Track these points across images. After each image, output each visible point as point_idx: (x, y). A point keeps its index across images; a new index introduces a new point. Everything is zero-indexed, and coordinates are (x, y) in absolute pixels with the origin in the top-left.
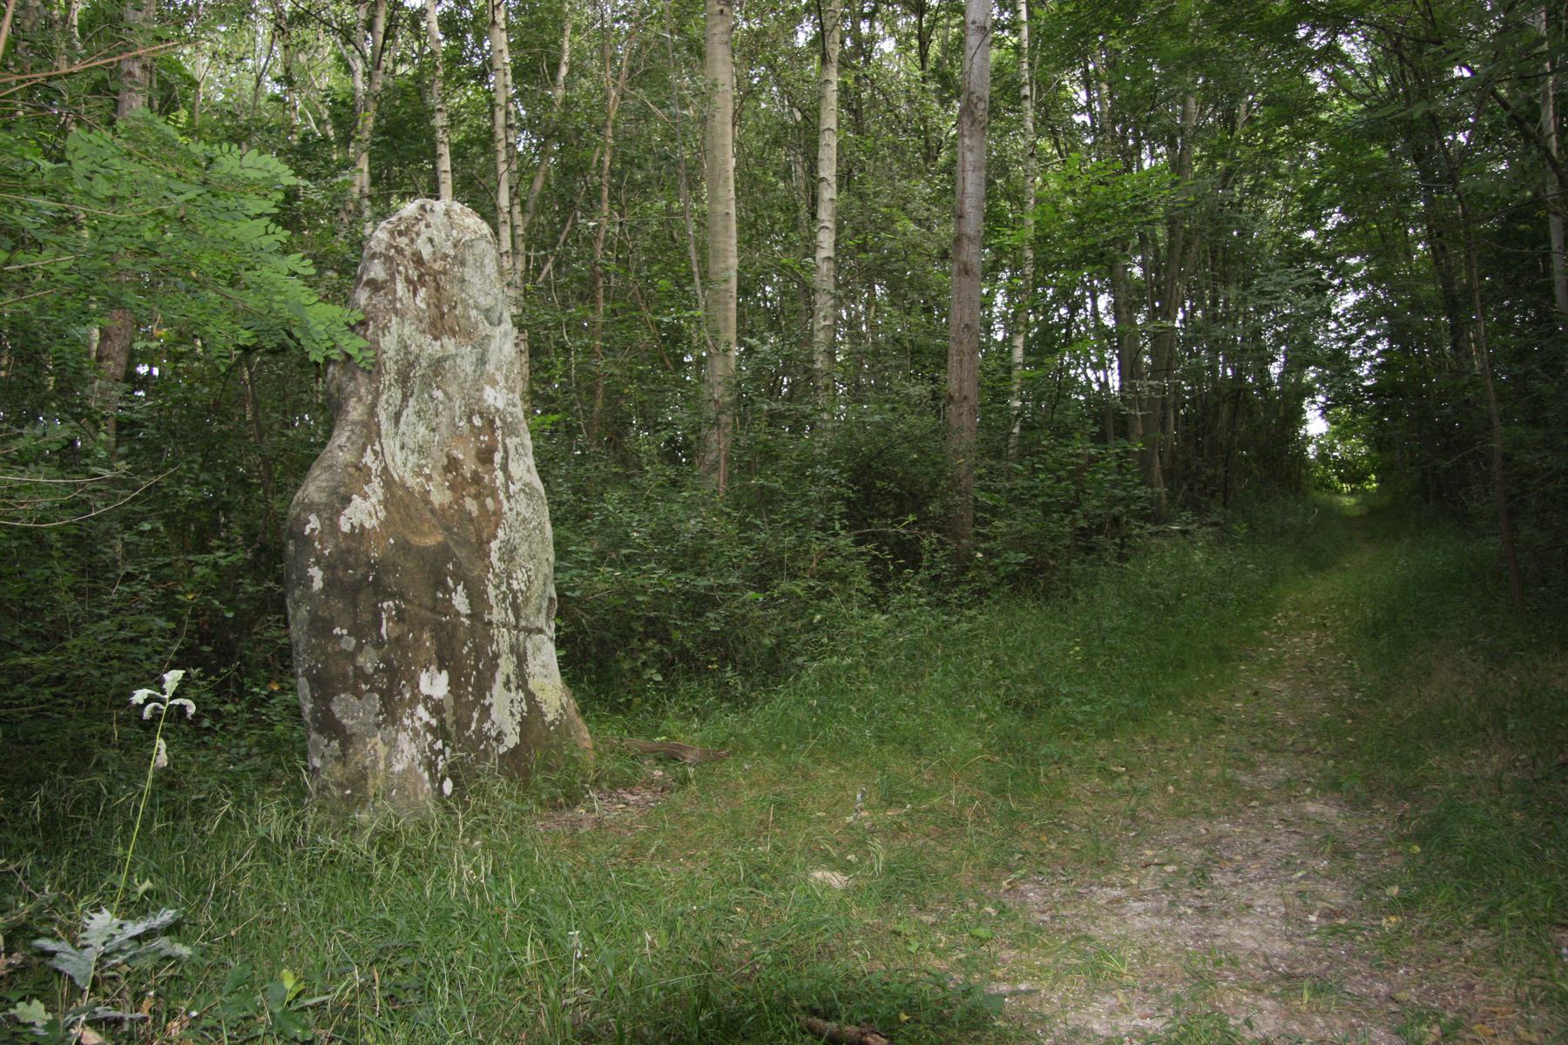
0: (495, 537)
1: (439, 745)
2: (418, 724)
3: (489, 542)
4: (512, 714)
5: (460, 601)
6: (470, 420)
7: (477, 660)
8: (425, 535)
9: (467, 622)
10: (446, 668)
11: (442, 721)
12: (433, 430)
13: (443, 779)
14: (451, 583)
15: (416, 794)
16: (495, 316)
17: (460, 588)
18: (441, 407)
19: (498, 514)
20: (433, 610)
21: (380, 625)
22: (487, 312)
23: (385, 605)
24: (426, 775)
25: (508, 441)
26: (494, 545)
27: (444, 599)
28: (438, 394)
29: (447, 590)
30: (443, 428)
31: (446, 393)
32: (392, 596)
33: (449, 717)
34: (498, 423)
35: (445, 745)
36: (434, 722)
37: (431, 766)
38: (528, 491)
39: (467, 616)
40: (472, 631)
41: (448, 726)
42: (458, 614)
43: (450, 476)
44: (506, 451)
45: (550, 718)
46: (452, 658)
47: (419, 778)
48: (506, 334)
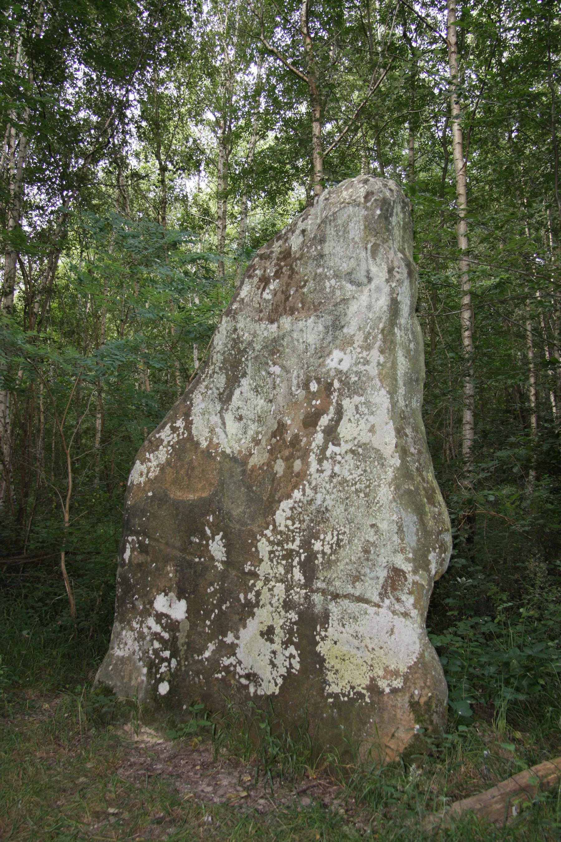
0: (289, 496)
1: (167, 654)
2: (145, 630)
3: (280, 501)
4: (274, 665)
5: (217, 549)
6: (306, 386)
7: (222, 601)
8: (195, 491)
9: (220, 567)
10: (185, 598)
11: (174, 639)
12: (271, 401)
13: (161, 680)
14: (208, 532)
15: (130, 679)
16: (361, 276)
17: (218, 538)
18: (278, 380)
19: (302, 476)
20: (183, 550)
21: (124, 551)
22: (350, 276)
23: (130, 539)
24: (145, 670)
25: (346, 403)
26: (286, 505)
27: (200, 544)
28: (276, 370)
29: (203, 535)
30: (280, 399)
31: (283, 367)
32: (137, 534)
33: (182, 637)
34: (336, 385)
35: (172, 656)
36: (166, 636)
37: (153, 667)
38: (362, 452)
39: (222, 562)
40: (223, 576)
41: (179, 643)
42: (212, 558)
43: (274, 440)
44: (339, 412)
45: (334, 689)
46: (194, 592)
47: (138, 670)
48: (378, 289)
